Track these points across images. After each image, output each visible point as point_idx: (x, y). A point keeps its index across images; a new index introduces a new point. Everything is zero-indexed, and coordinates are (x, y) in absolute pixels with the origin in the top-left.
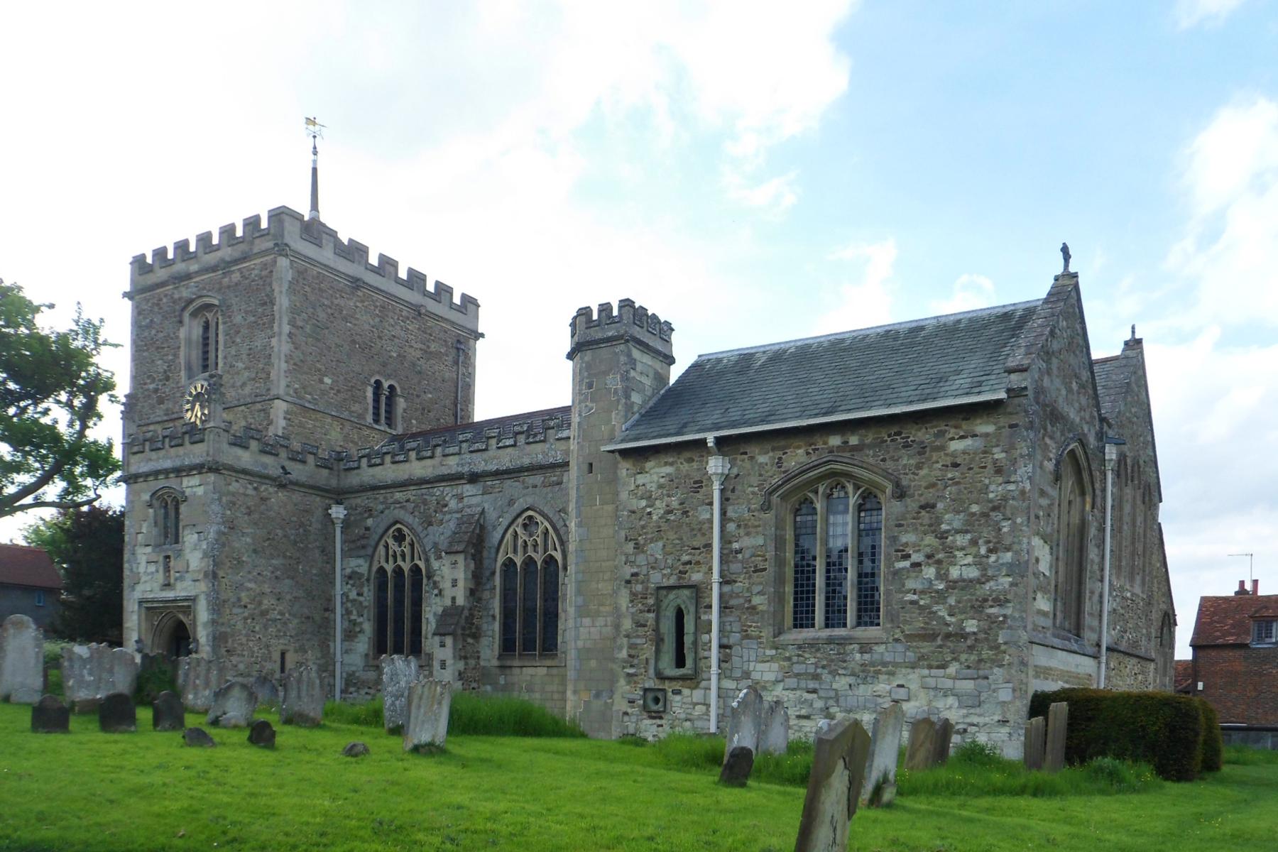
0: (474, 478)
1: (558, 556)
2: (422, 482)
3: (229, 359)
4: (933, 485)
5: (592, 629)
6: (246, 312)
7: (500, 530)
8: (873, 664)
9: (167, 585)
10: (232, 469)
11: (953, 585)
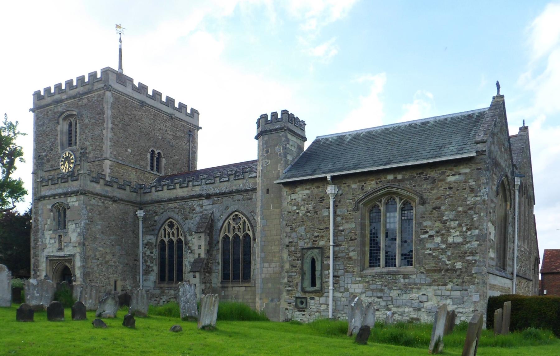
0: (208, 197)
1: (251, 233)
2: (182, 199)
3: (82, 141)
4: (439, 198)
5: (269, 269)
6: (90, 118)
7: (221, 222)
8: (410, 284)
9: (60, 249)
10: (92, 193)
11: (450, 246)
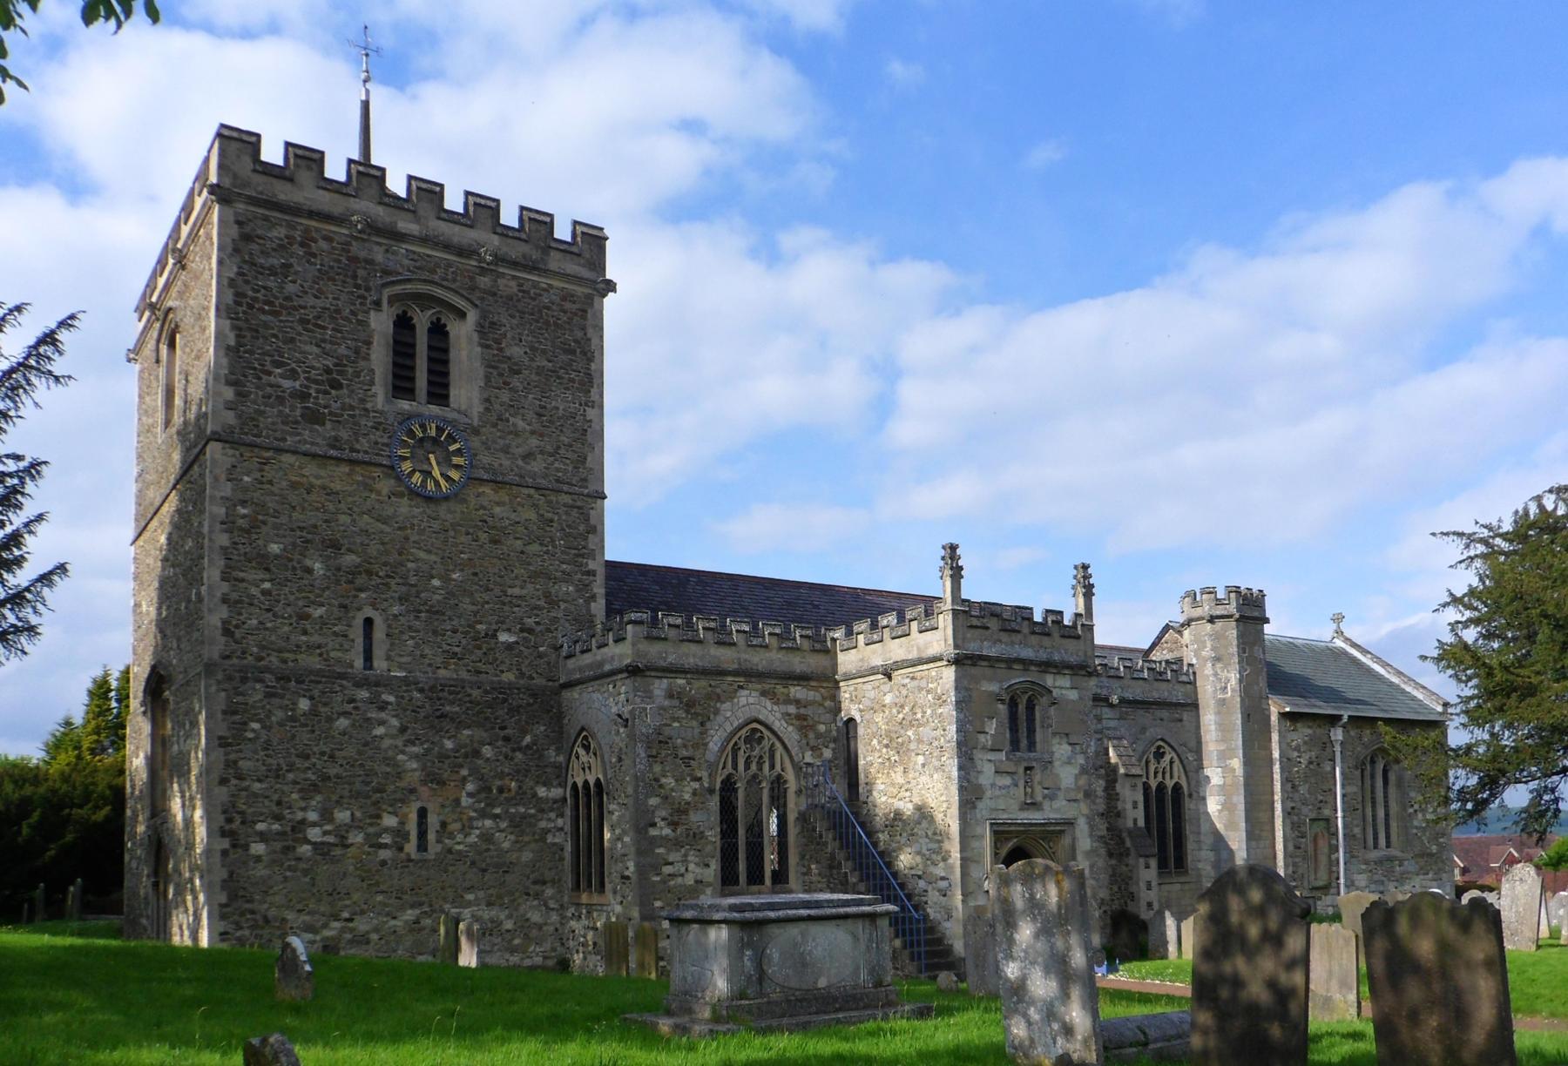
9: (1034, 805)
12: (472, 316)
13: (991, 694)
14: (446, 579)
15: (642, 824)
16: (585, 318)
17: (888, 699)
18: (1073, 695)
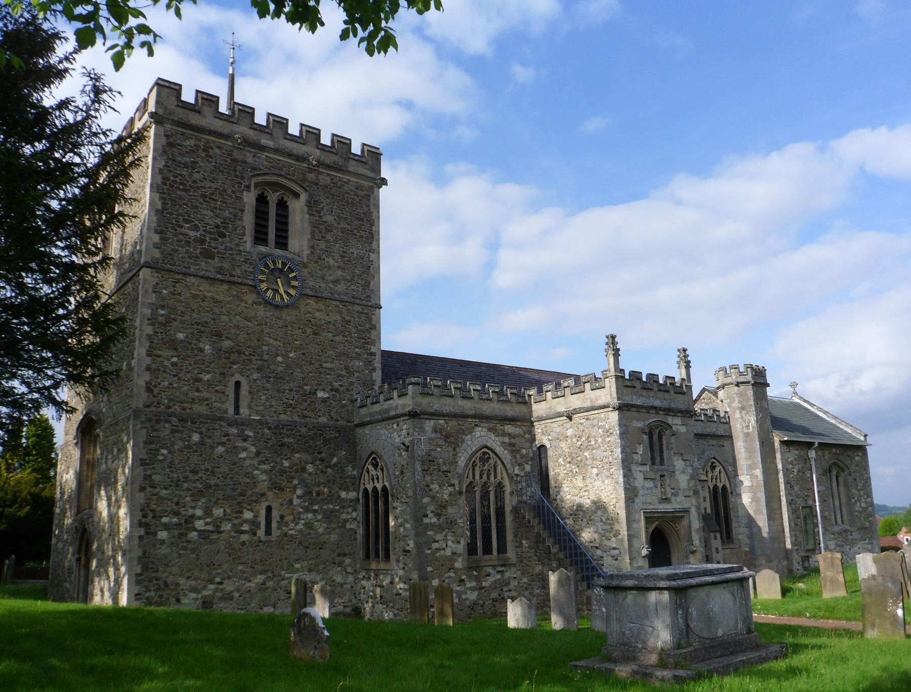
9: (666, 500)
12: (304, 197)
13: (639, 428)
14: (286, 357)
15: (418, 515)
16: (369, 200)
17: (569, 433)
18: (683, 429)
